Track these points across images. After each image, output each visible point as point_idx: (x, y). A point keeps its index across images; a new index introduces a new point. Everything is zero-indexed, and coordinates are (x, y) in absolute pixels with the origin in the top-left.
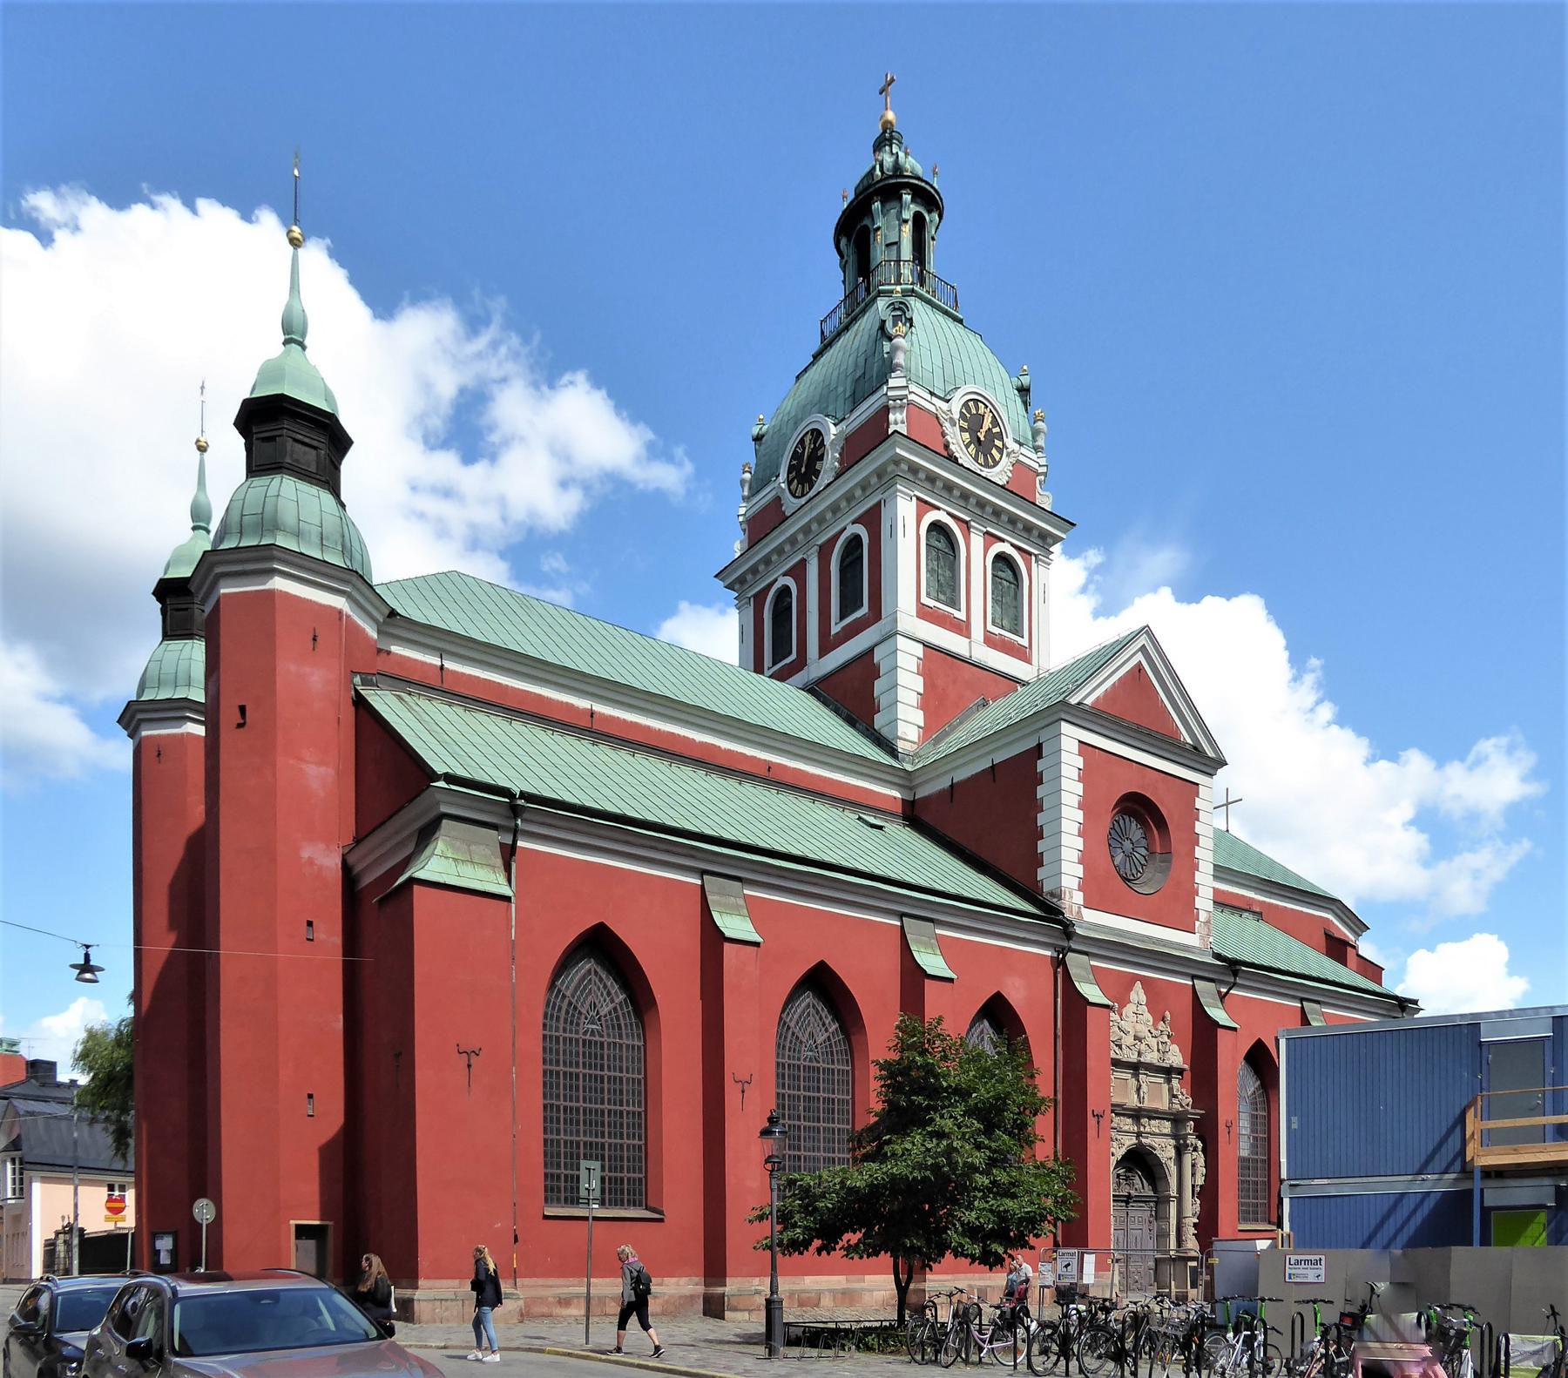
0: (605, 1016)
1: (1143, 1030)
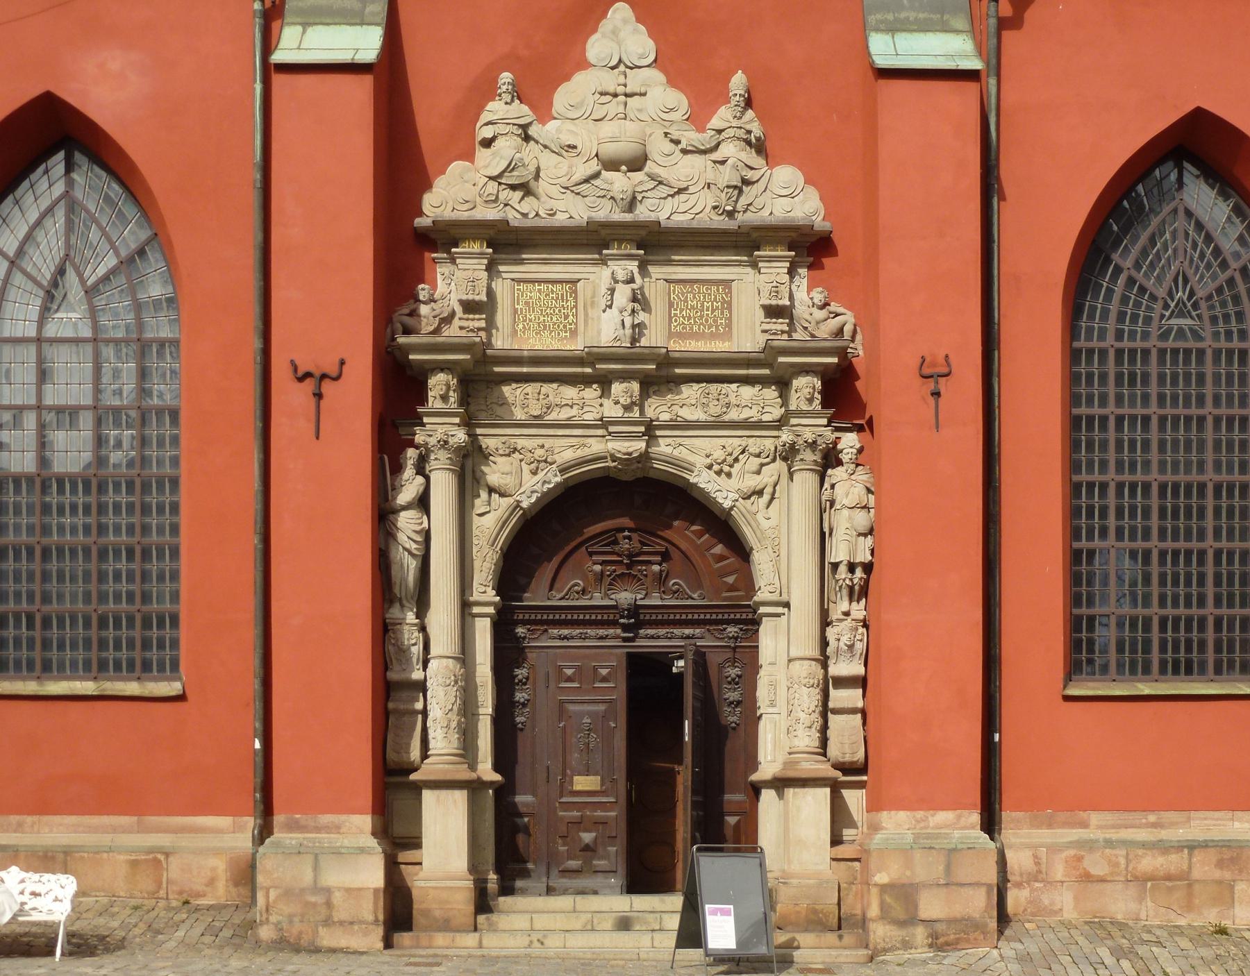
0: (1210, 297)
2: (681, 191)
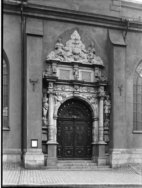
1: (77, 50)
2: (84, 59)
